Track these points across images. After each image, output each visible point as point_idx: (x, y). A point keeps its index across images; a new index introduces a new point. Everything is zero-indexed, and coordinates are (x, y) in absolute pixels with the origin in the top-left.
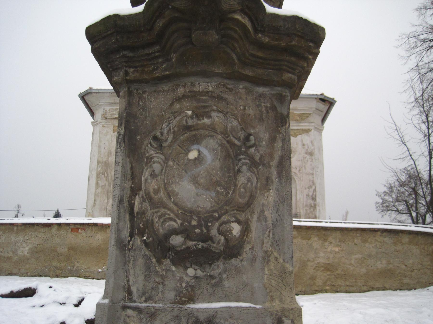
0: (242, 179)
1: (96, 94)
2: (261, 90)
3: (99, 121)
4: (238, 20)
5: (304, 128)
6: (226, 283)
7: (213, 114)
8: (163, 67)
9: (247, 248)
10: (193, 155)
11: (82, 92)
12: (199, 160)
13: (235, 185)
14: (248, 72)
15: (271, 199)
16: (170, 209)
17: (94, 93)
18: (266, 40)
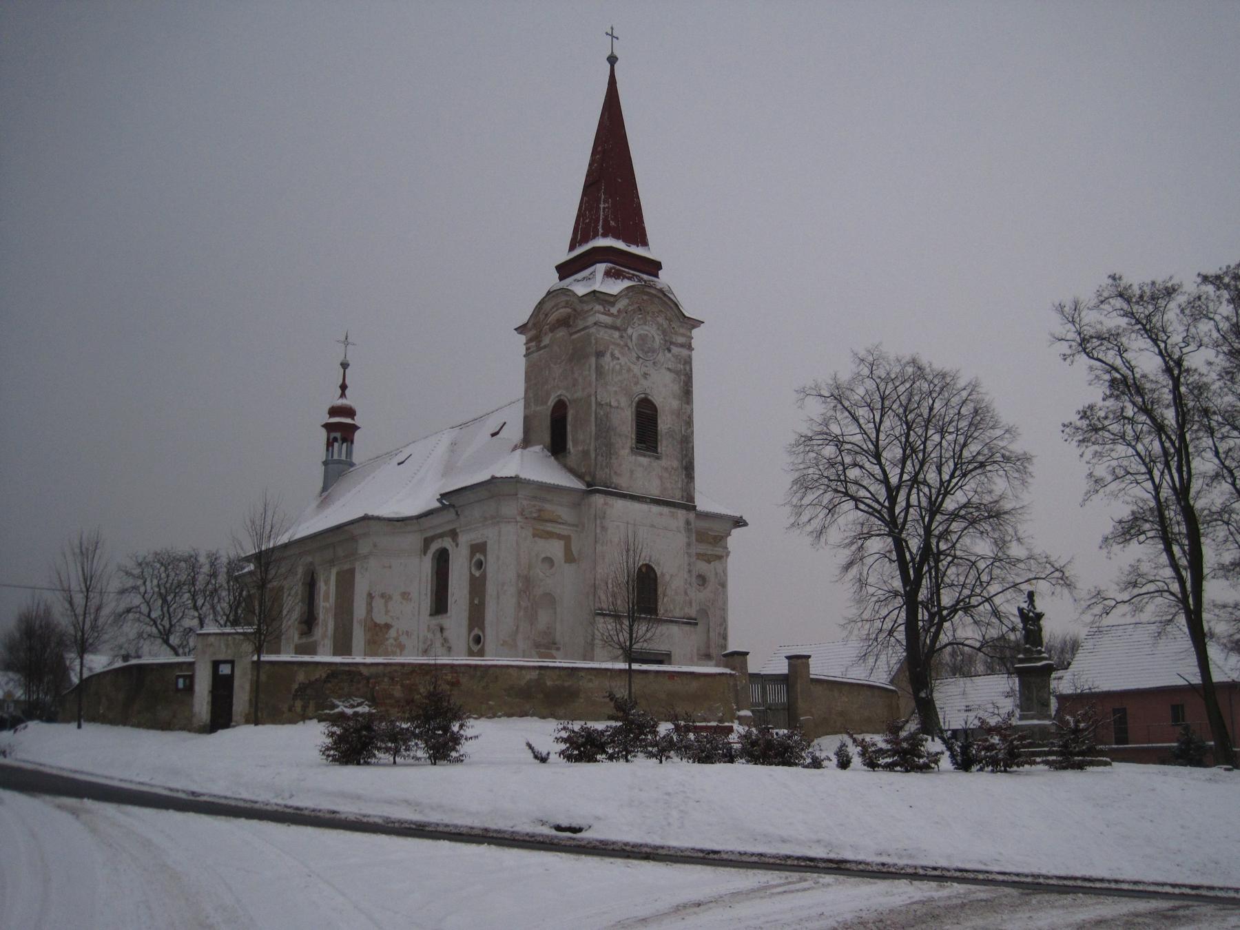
5: (717, 553)
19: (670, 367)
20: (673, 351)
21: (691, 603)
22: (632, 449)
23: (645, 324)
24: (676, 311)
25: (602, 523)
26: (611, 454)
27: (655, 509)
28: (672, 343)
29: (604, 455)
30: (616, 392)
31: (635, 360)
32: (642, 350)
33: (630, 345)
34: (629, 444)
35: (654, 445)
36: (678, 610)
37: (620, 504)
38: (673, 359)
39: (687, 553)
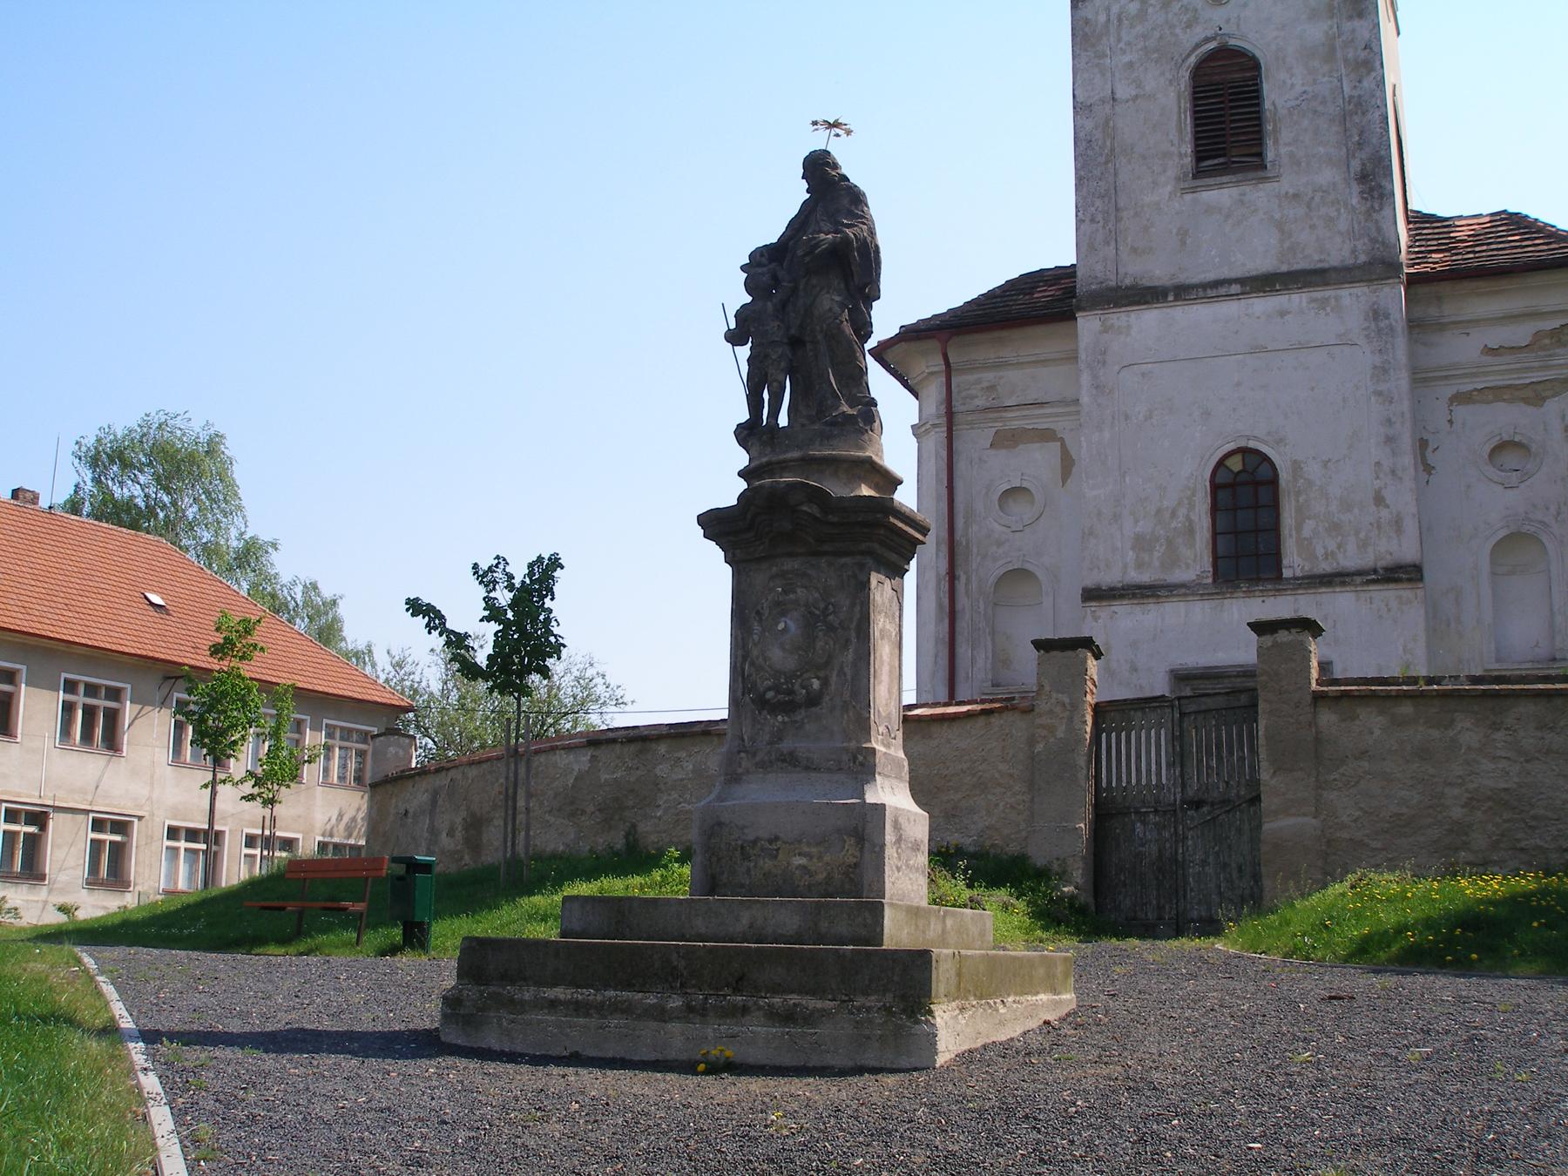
0: (820, 644)
2: (843, 560)
3: (931, 423)
4: (805, 512)
6: (807, 727)
7: (799, 590)
9: (827, 698)
10: (781, 626)
12: (785, 630)
13: (814, 649)
14: (826, 547)
15: (850, 656)
16: (767, 671)
21: (1398, 523)
25: (1095, 377)
26: (1117, 209)
27: (1262, 305)
29: (1099, 217)
30: (1131, 64)
34: (1171, 173)
35: (1254, 150)
36: (1351, 547)
37: (1145, 322)
39: (1379, 394)
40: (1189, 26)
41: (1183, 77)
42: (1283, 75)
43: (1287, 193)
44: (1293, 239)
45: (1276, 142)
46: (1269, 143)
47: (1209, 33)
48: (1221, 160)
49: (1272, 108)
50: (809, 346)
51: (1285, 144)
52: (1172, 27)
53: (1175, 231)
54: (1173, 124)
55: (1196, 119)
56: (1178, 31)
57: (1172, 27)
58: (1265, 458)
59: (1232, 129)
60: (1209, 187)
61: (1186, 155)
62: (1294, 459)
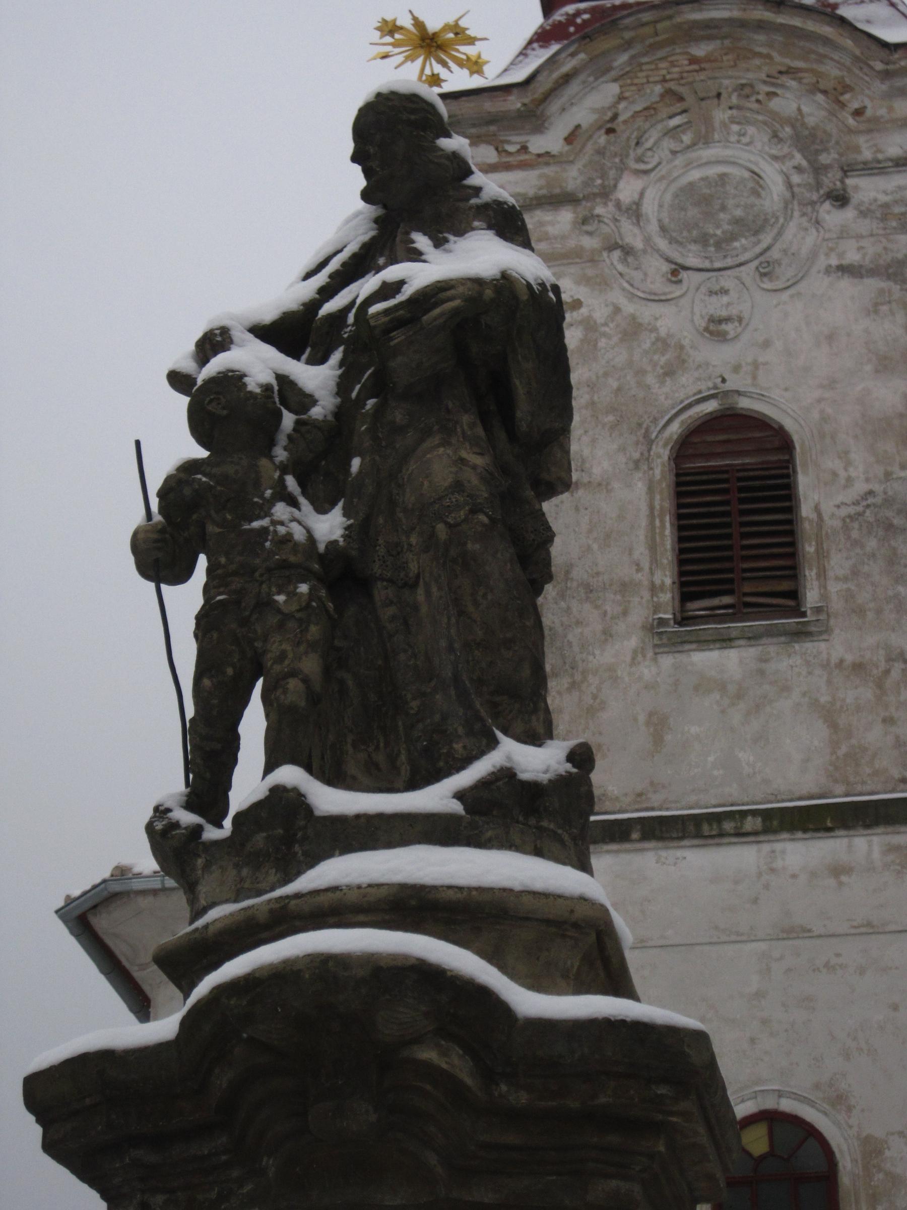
1: (150, 899)
4: (428, 1065)
8: (245, 1191)
11: (76, 893)
17: (143, 893)
18: (522, 1098)
19: (852, 257)
20: (856, 198)
22: (655, 628)
23: (704, 139)
24: (849, 43)
28: (847, 170)
31: (658, 285)
32: (703, 240)
33: (632, 235)
34: (639, 614)
35: (785, 586)
38: (865, 226)
40: (669, 373)
41: (659, 456)
42: (835, 464)
43: (842, 661)
44: (854, 741)
45: (822, 574)
46: (810, 574)
47: (705, 386)
48: (727, 600)
49: (813, 516)
50: (381, 592)
51: (837, 579)
52: (641, 372)
53: (642, 718)
54: (641, 534)
55: (681, 528)
56: (650, 379)
57: (641, 372)
58: (811, 1132)
59: (745, 547)
60: (703, 643)
61: (662, 587)
62: (864, 1134)
